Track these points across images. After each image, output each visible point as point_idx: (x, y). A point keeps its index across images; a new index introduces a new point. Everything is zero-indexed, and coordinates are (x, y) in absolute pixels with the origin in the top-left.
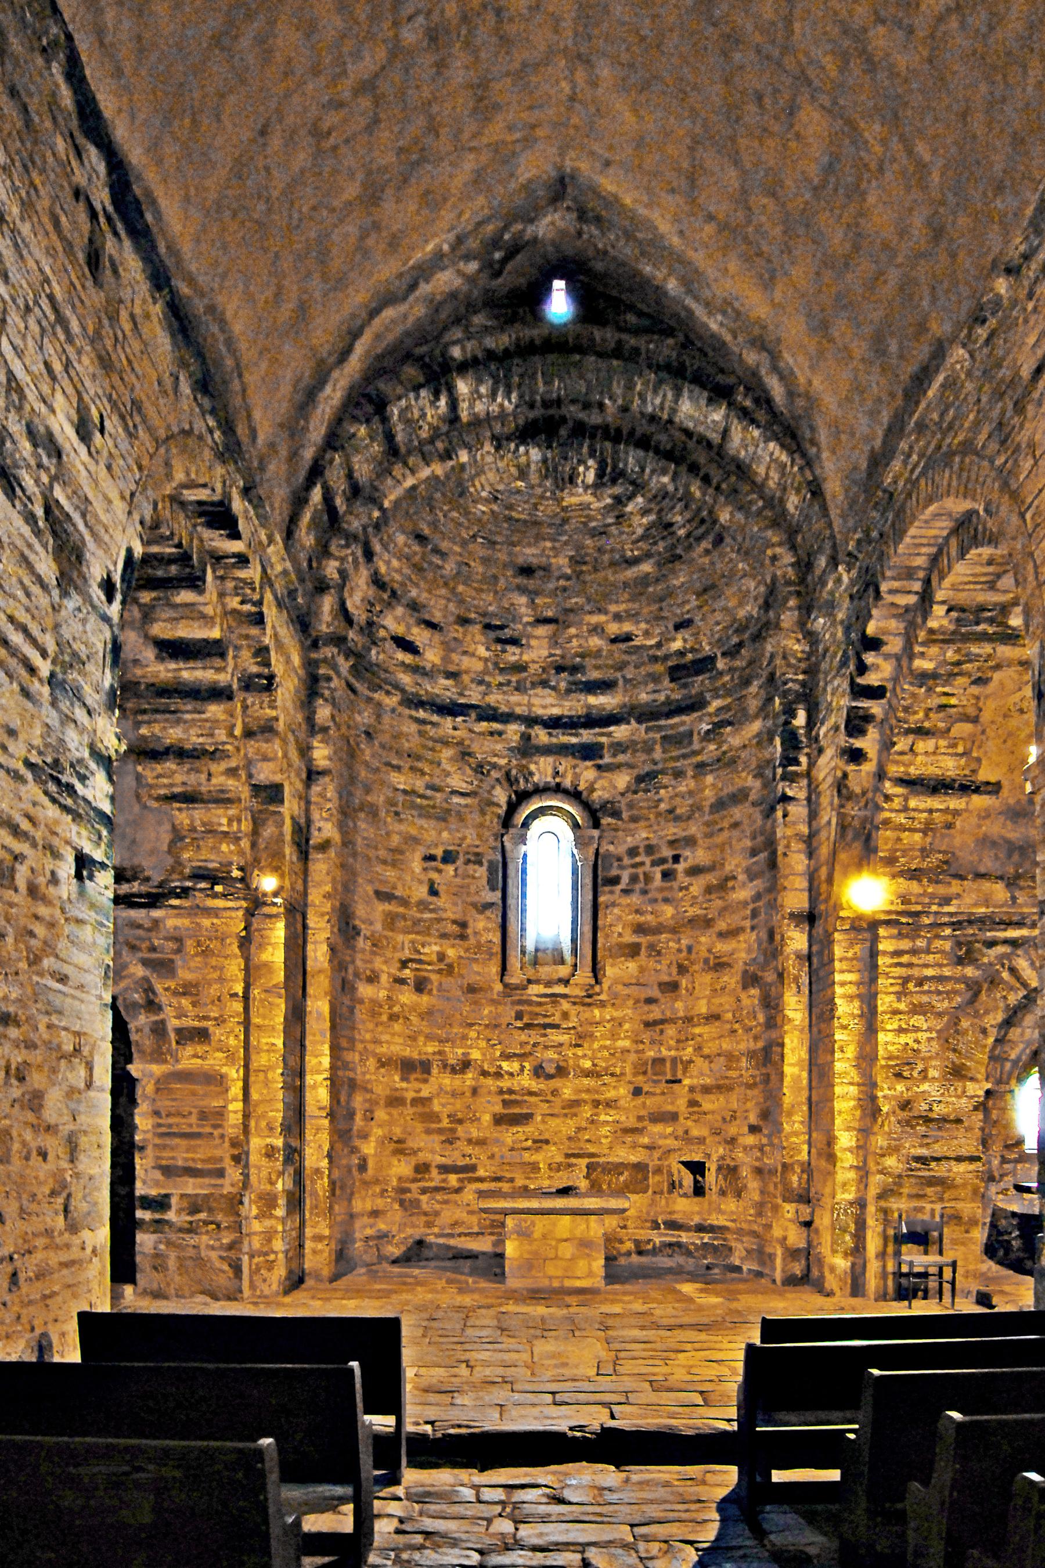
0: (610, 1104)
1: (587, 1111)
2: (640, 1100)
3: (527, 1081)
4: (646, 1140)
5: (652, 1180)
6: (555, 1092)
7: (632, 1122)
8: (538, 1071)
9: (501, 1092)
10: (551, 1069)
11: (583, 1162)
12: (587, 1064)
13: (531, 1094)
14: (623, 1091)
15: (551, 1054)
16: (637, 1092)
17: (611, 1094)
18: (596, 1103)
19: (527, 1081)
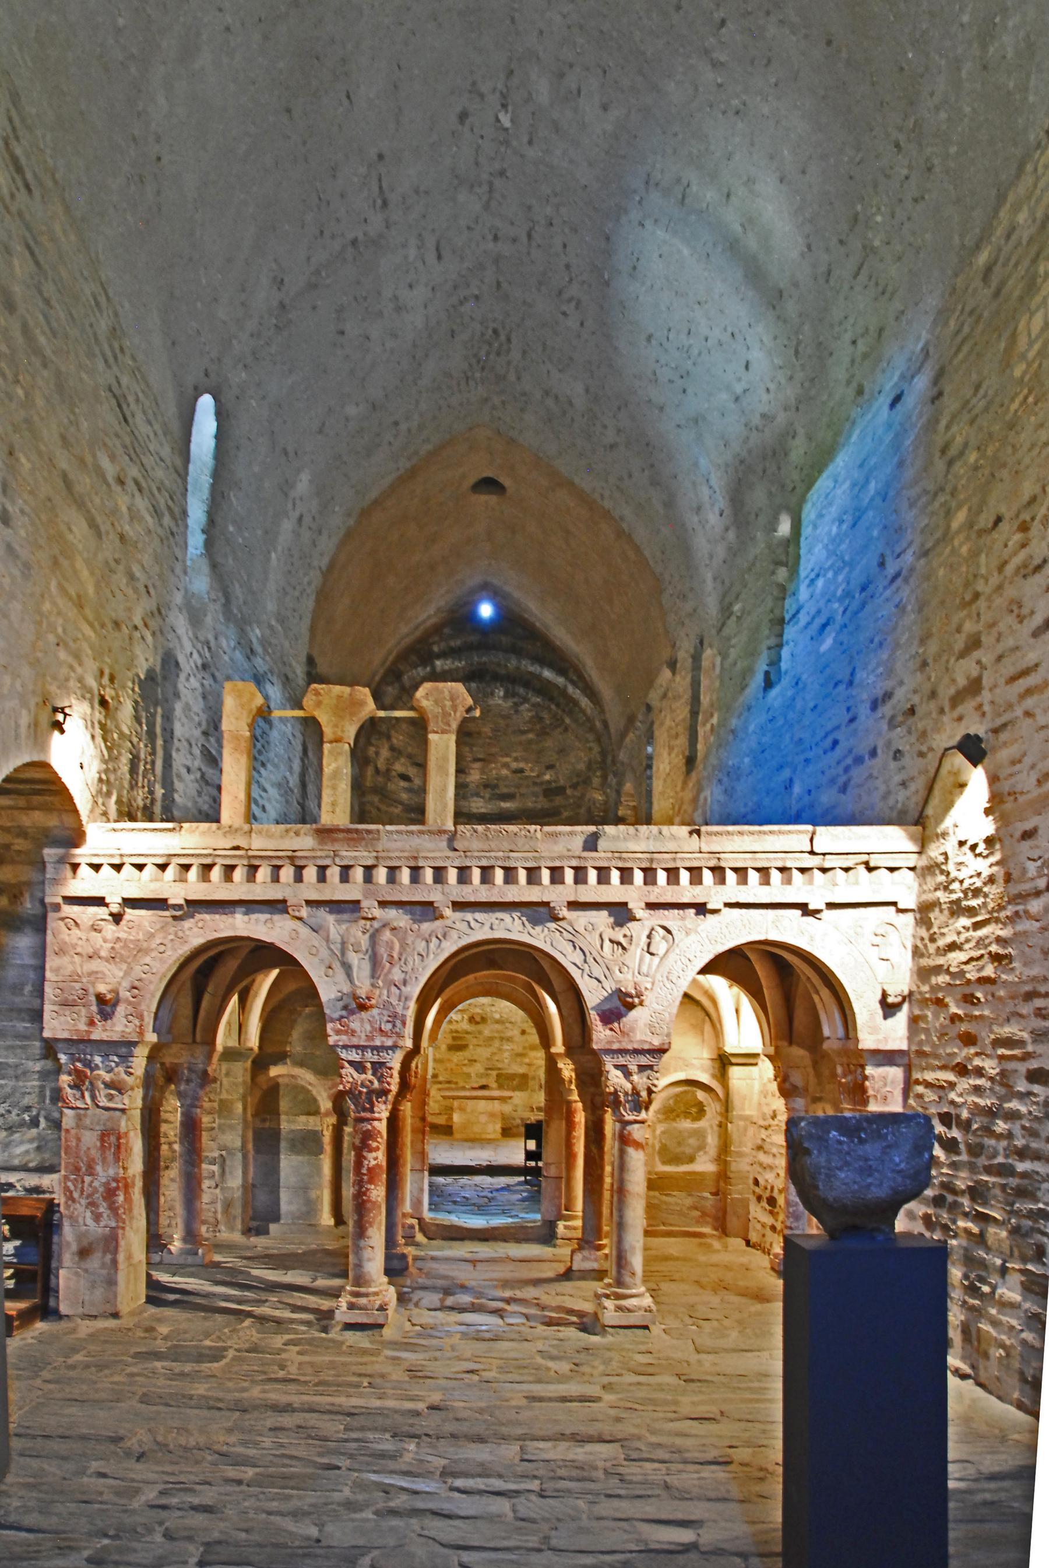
0: (509, 1039)
1: (497, 1043)
2: (525, 1037)
3: (465, 1026)
4: (527, 1060)
5: (531, 1083)
6: (480, 1032)
7: (520, 1050)
8: (472, 1020)
9: (452, 1031)
10: (478, 1019)
11: (494, 1073)
12: (497, 1016)
13: (467, 1033)
14: (515, 1033)
15: (478, 1010)
16: (523, 1032)
17: (509, 1034)
18: (502, 1039)
19: (465, 1026)
